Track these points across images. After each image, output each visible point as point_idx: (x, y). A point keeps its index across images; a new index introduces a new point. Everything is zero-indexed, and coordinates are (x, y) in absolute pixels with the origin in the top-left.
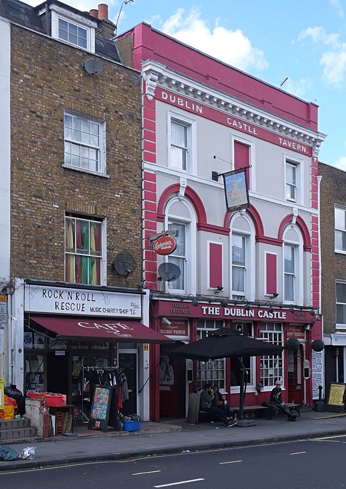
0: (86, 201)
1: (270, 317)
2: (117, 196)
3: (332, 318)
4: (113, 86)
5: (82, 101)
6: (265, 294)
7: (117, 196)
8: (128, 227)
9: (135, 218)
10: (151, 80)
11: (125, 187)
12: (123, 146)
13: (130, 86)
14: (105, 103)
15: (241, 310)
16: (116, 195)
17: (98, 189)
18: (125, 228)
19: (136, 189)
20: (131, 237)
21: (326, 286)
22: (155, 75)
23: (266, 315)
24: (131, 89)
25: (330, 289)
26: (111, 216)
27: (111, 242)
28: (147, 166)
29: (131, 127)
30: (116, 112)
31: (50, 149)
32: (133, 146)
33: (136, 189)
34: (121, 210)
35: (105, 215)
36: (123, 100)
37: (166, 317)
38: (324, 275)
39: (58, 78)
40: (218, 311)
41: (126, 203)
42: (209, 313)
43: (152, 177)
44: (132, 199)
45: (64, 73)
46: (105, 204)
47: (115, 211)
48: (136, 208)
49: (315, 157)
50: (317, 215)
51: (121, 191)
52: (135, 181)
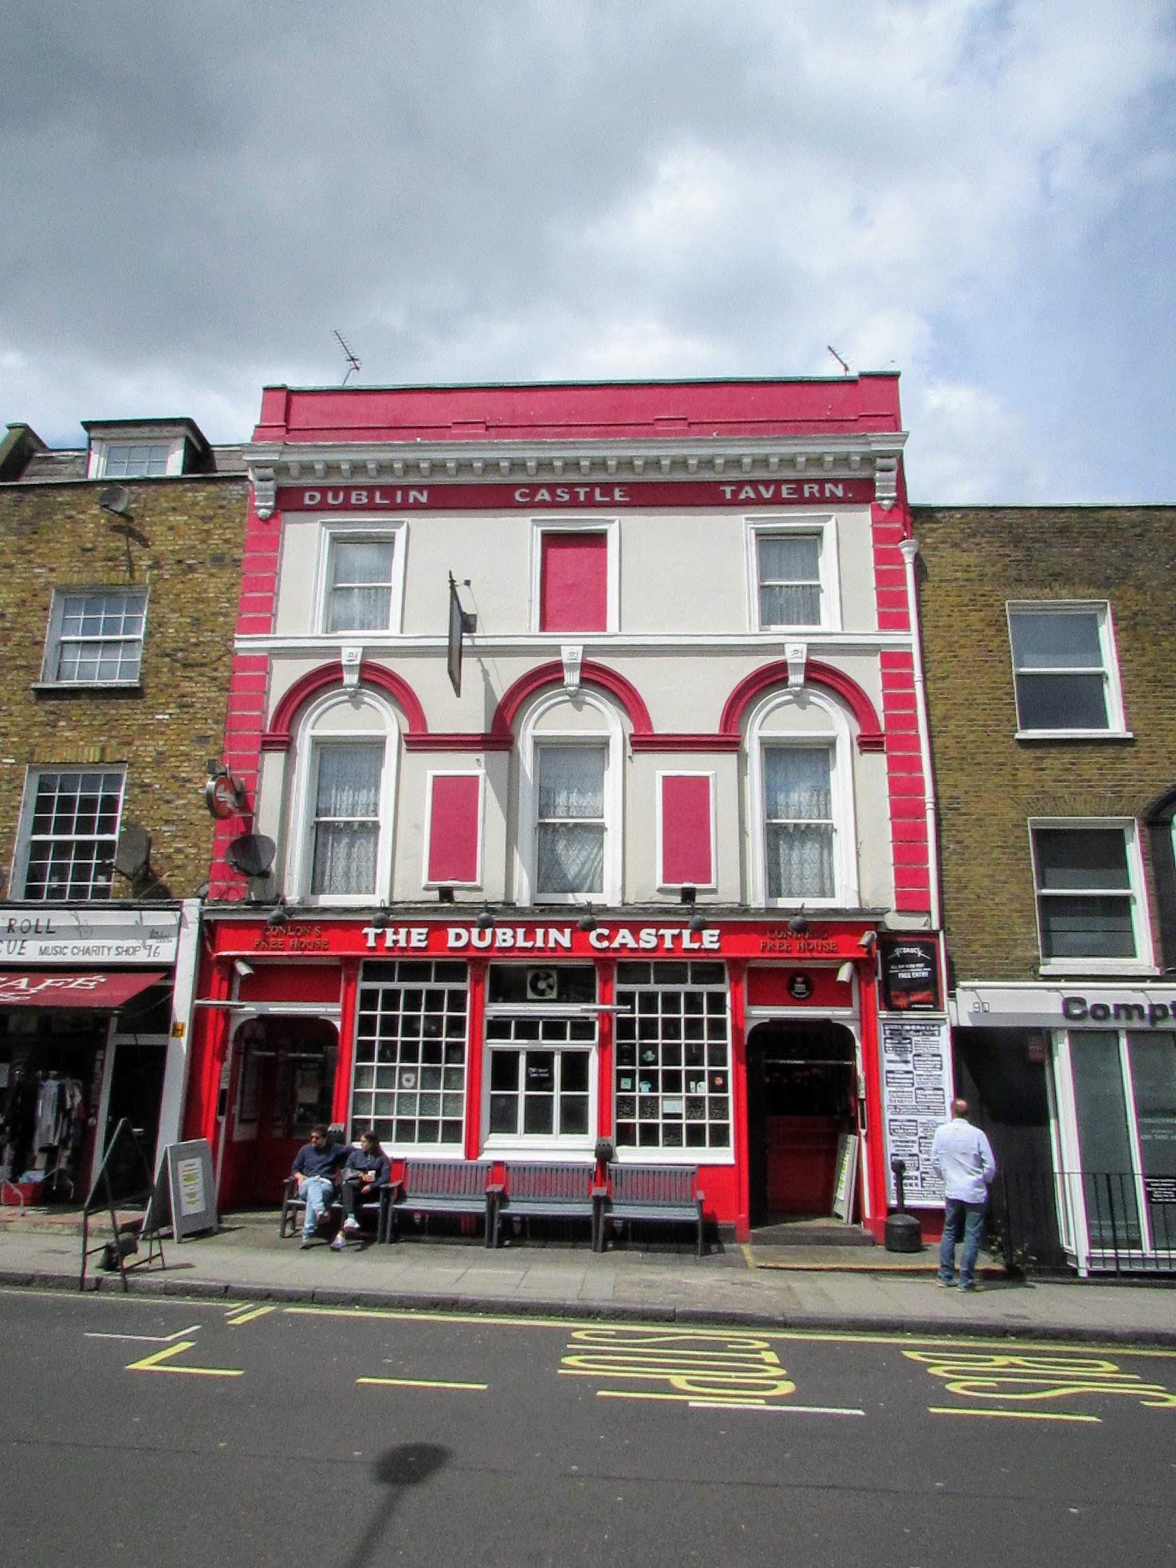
0: (81, 740)
1: (643, 945)
2: (160, 717)
3: (1016, 940)
4: (178, 518)
5: (99, 564)
6: (659, 883)
7: (160, 717)
8: (183, 775)
9: (203, 753)
10: (261, 480)
11: (183, 696)
12: (188, 620)
13: (222, 507)
14: (153, 553)
15: (515, 932)
16: (158, 717)
17: (113, 712)
18: (174, 777)
19: (213, 695)
20: (189, 792)
21: (976, 842)
22: (267, 467)
23: (623, 941)
24: (222, 511)
25: (998, 850)
26: (141, 759)
27: (133, 811)
28: (244, 644)
29: (214, 580)
30: (180, 562)
31: (12, 663)
32: (214, 614)
33: (213, 695)
34: (169, 742)
35: (125, 759)
36: (199, 536)
37: (243, 959)
38: (963, 811)
39: (48, 541)
40: (423, 937)
41: (184, 728)
42: (389, 943)
43: (262, 663)
44: (199, 716)
45: (63, 530)
46: (129, 739)
47: (148, 749)
48: (211, 732)
49: (883, 499)
50: (910, 645)
51: (173, 705)
52: (215, 679)
